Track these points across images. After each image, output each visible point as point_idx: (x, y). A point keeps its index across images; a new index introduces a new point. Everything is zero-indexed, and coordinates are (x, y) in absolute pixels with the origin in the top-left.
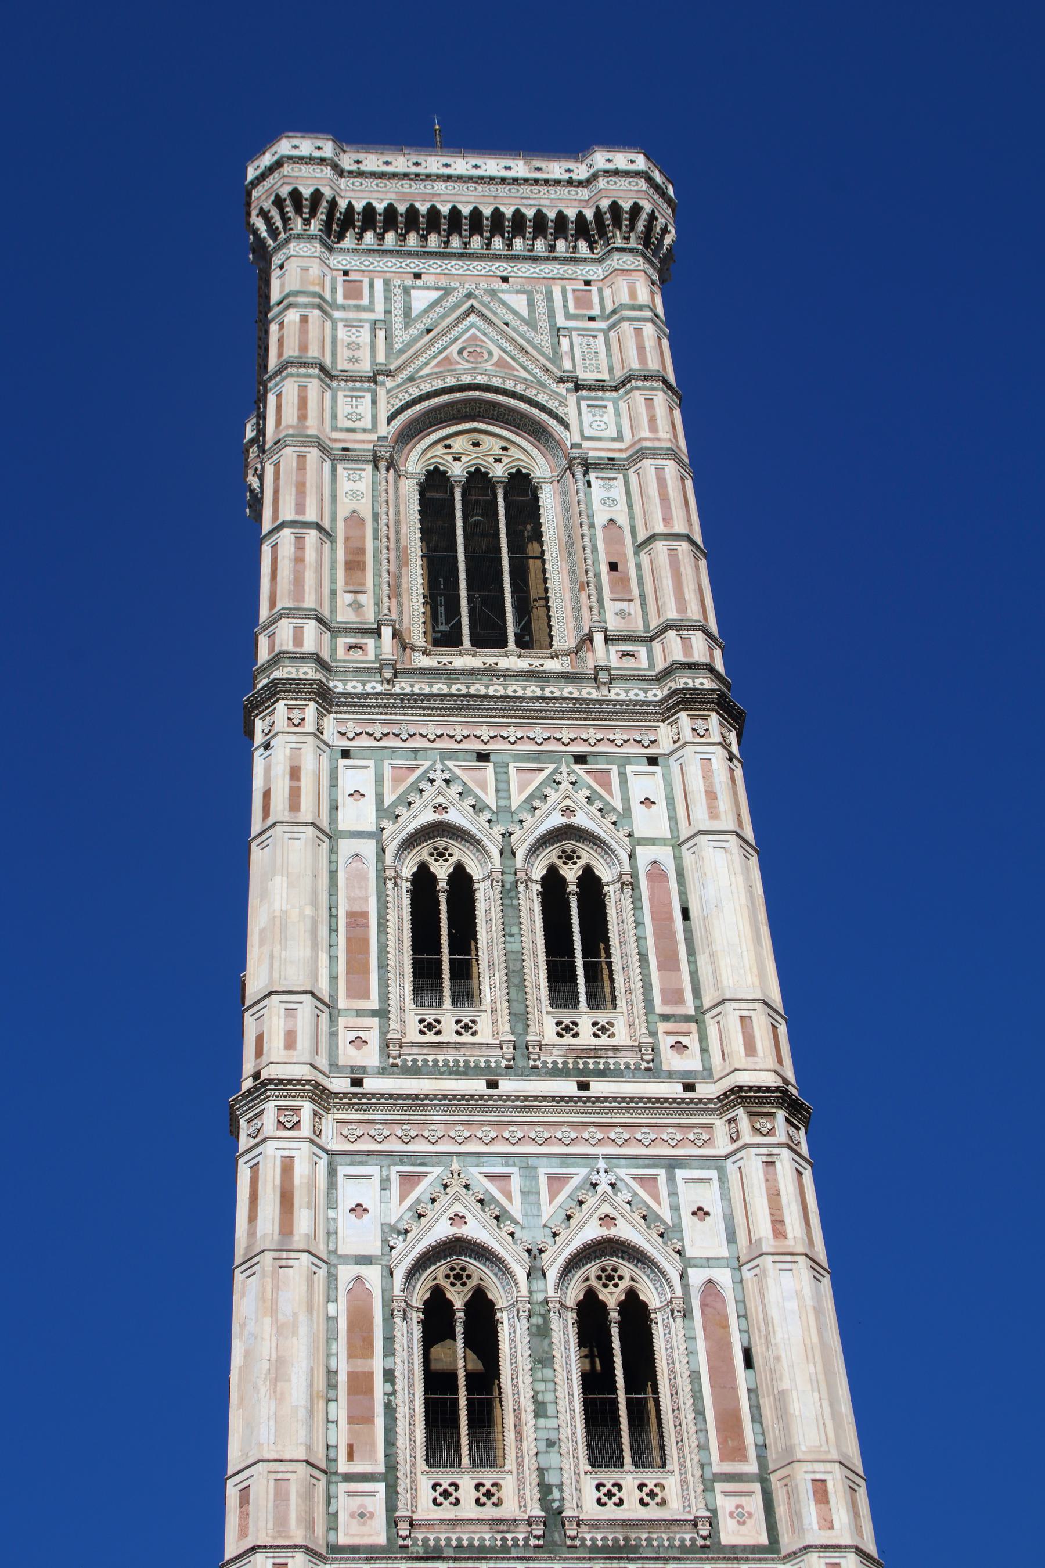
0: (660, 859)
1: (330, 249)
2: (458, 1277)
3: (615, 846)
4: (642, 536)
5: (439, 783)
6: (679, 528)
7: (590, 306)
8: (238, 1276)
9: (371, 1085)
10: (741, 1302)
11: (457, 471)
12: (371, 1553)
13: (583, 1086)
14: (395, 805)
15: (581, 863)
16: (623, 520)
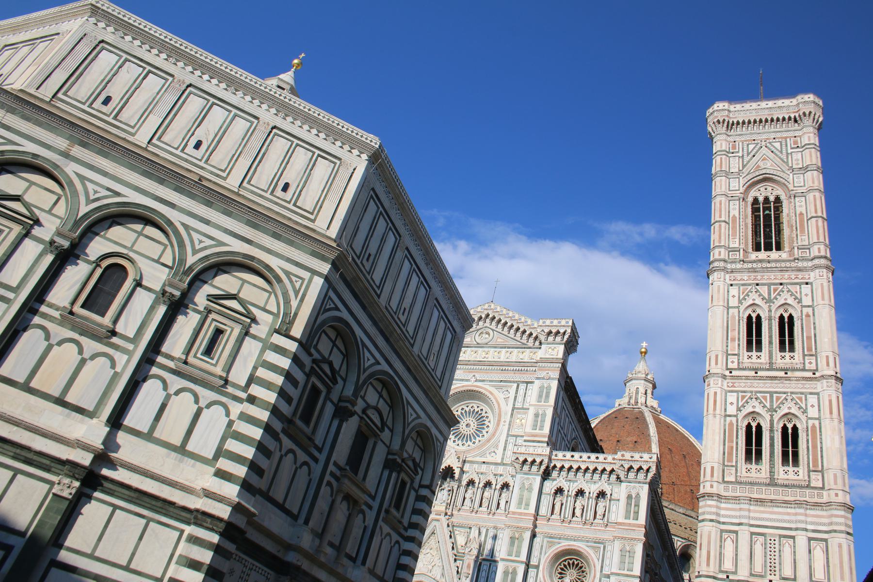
0: (809, 311)
1: (728, 135)
2: (754, 420)
3: (797, 308)
4: (809, 217)
5: (754, 293)
6: (820, 214)
7: (797, 144)
8: (705, 419)
9: (734, 373)
10: (820, 428)
11: (761, 199)
12: (731, 482)
13: (786, 373)
14: (742, 300)
15: (789, 313)
16: (804, 212)
